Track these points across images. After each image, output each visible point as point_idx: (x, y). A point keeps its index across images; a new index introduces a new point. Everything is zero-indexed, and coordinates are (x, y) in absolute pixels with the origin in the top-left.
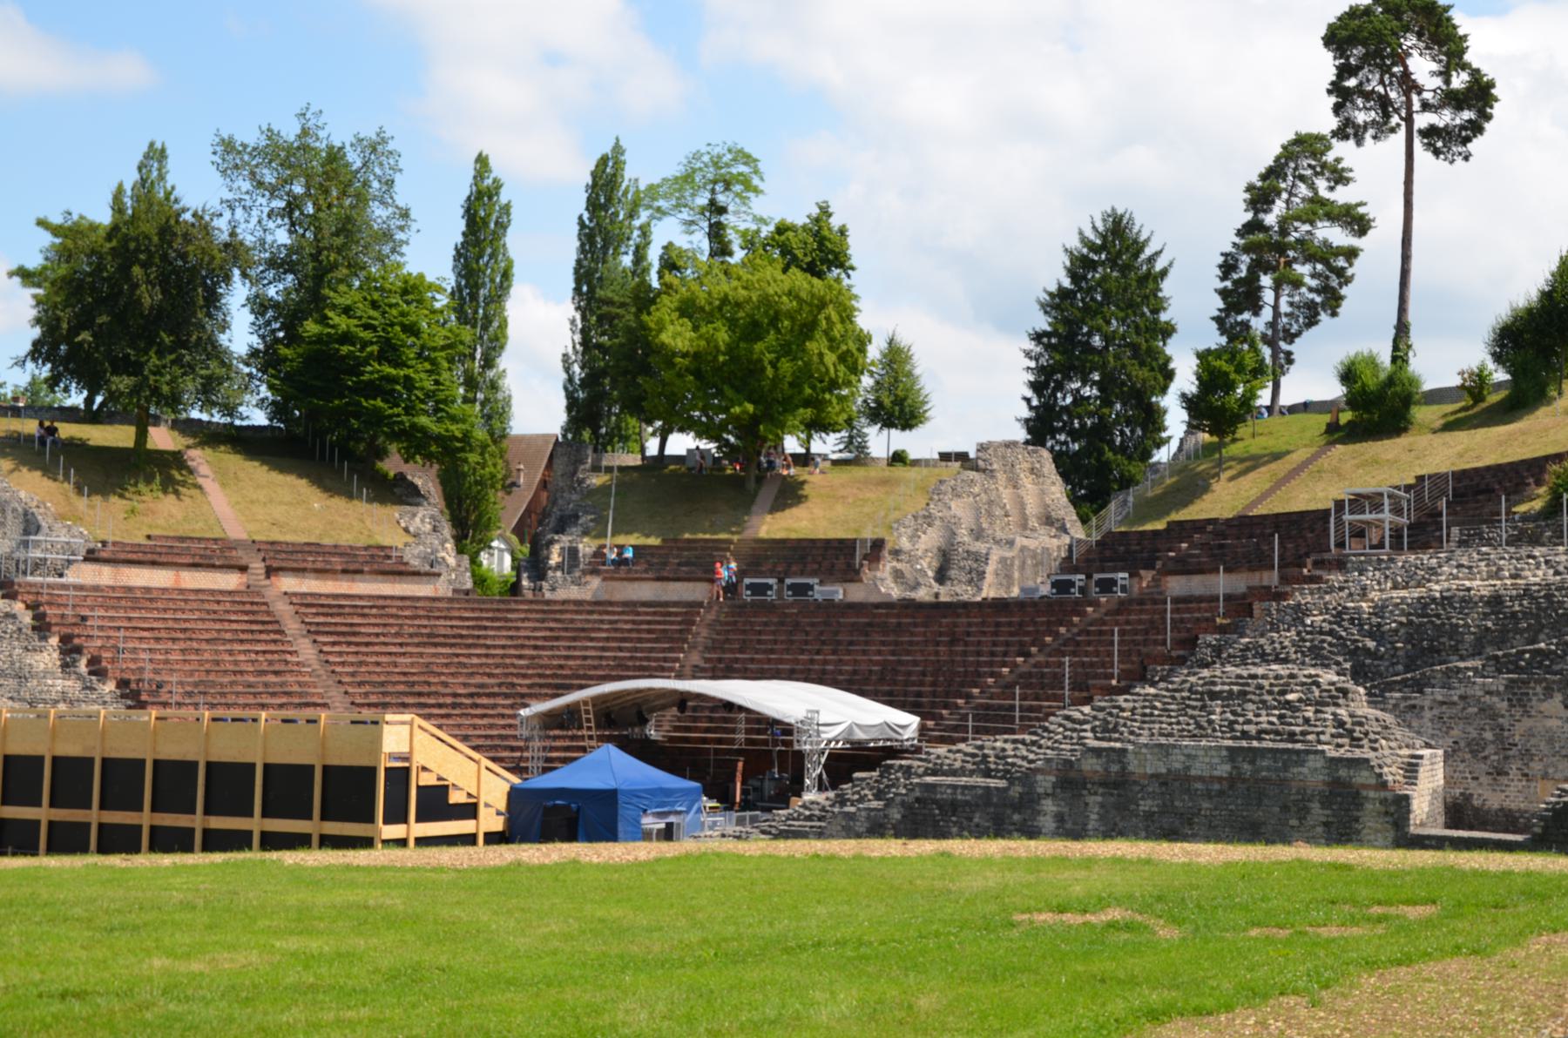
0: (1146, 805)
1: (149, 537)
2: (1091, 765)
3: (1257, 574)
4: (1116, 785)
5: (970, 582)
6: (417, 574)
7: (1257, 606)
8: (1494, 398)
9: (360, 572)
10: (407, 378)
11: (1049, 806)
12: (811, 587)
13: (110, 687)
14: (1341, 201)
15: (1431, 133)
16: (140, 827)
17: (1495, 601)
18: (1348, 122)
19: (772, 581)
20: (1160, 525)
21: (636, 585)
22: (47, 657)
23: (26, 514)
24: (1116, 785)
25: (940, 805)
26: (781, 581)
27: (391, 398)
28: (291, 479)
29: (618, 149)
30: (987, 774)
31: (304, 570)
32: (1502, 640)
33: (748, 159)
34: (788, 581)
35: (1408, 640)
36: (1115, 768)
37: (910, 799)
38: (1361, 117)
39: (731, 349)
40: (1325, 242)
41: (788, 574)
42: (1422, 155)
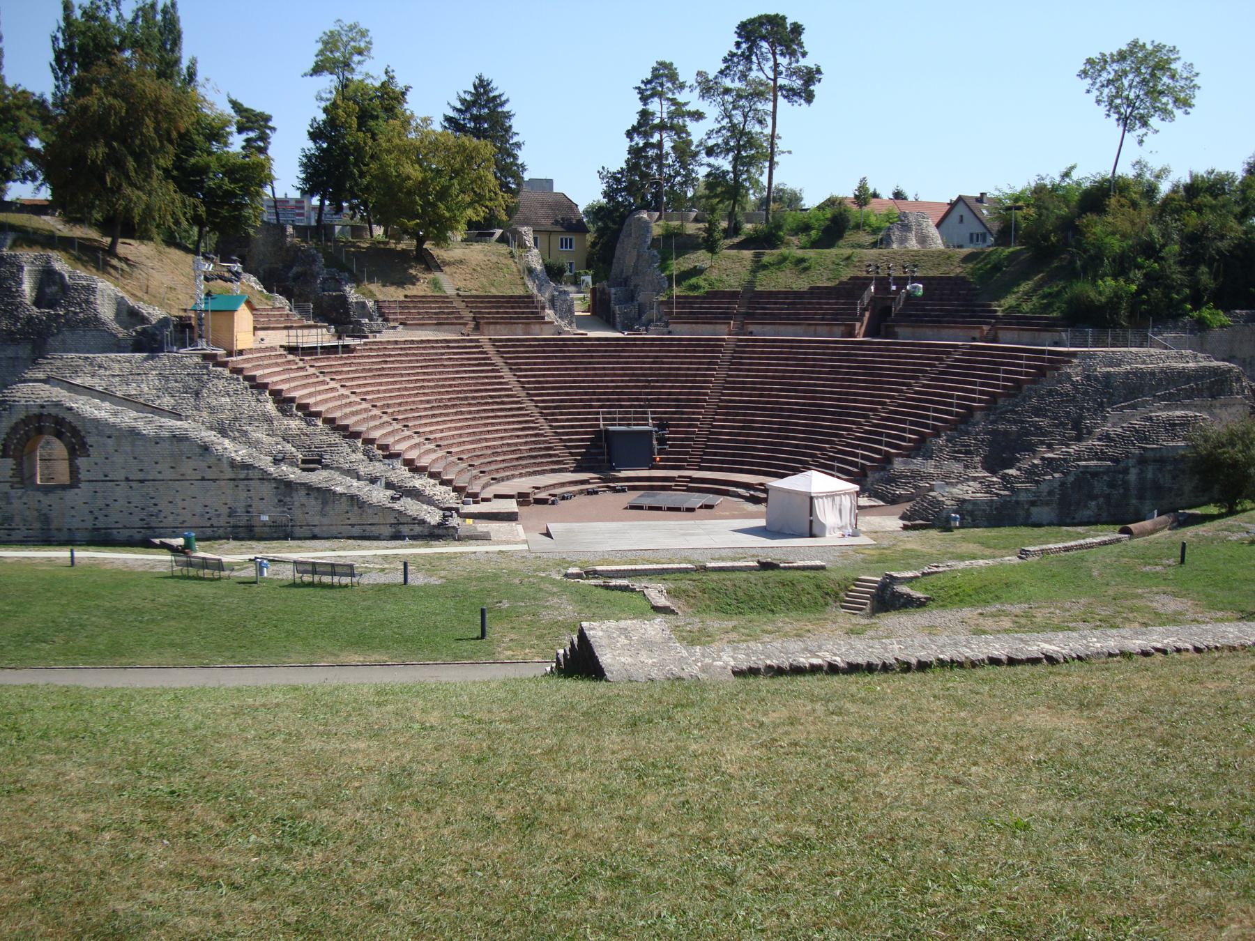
2: (1150, 454)
7: (1048, 373)
13: (320, 423)
22: (270, 407)
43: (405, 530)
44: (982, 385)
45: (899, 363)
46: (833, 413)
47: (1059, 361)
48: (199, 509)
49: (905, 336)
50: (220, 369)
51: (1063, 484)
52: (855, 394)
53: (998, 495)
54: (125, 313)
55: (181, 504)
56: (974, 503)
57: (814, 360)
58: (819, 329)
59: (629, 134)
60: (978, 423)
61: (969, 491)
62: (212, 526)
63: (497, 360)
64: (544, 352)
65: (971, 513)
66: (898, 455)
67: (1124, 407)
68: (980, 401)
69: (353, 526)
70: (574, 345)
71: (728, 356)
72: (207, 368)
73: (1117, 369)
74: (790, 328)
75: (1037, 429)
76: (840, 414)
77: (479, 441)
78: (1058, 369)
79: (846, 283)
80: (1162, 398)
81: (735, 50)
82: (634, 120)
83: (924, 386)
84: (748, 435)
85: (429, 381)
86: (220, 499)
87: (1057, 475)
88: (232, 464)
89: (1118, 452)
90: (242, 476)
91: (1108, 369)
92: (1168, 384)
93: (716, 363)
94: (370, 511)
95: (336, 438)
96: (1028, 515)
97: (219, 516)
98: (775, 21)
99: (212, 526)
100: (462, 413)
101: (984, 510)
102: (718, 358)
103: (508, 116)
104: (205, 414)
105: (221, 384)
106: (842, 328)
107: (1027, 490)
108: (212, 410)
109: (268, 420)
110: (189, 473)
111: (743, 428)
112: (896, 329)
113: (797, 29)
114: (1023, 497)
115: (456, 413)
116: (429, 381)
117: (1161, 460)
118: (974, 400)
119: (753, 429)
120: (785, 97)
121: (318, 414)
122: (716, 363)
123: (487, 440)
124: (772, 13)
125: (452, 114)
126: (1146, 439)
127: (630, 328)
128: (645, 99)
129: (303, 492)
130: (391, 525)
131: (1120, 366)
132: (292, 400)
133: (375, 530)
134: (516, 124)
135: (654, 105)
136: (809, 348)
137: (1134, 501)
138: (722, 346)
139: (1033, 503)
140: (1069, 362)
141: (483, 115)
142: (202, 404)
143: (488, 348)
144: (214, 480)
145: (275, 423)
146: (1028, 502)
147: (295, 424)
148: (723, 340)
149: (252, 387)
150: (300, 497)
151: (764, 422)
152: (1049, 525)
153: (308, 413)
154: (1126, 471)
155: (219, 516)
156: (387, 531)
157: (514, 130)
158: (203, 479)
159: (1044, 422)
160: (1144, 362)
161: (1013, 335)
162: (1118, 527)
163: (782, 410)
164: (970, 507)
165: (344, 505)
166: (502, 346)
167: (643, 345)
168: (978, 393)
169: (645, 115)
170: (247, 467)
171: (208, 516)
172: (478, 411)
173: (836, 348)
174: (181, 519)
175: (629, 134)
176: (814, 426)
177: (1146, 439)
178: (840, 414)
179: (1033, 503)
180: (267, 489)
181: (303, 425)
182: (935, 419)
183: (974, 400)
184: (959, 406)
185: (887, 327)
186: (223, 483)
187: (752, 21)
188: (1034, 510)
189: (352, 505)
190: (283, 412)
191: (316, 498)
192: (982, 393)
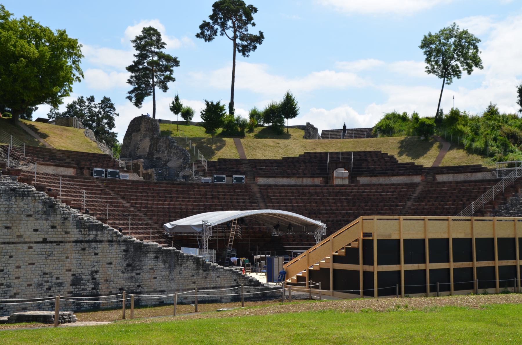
3: (301, 179)
14: (166, 53)
19: (104, 170)
48: (36, 279)
55: (14, 272)
90: (92, 237)
97: (60, 284)
110: (29, 235)
112: (358, 178)
129: (151, 256)
133: (217, 294)
144: (58, 243)
155: (60, 284)
156: (227, 293)
158: (45, 241)
165: (189, 268)
171: (46, 286)
174: (13, 291)
180: (115, 253)
186: (68, 245)
189: (198, 269)
191: (165, 262)
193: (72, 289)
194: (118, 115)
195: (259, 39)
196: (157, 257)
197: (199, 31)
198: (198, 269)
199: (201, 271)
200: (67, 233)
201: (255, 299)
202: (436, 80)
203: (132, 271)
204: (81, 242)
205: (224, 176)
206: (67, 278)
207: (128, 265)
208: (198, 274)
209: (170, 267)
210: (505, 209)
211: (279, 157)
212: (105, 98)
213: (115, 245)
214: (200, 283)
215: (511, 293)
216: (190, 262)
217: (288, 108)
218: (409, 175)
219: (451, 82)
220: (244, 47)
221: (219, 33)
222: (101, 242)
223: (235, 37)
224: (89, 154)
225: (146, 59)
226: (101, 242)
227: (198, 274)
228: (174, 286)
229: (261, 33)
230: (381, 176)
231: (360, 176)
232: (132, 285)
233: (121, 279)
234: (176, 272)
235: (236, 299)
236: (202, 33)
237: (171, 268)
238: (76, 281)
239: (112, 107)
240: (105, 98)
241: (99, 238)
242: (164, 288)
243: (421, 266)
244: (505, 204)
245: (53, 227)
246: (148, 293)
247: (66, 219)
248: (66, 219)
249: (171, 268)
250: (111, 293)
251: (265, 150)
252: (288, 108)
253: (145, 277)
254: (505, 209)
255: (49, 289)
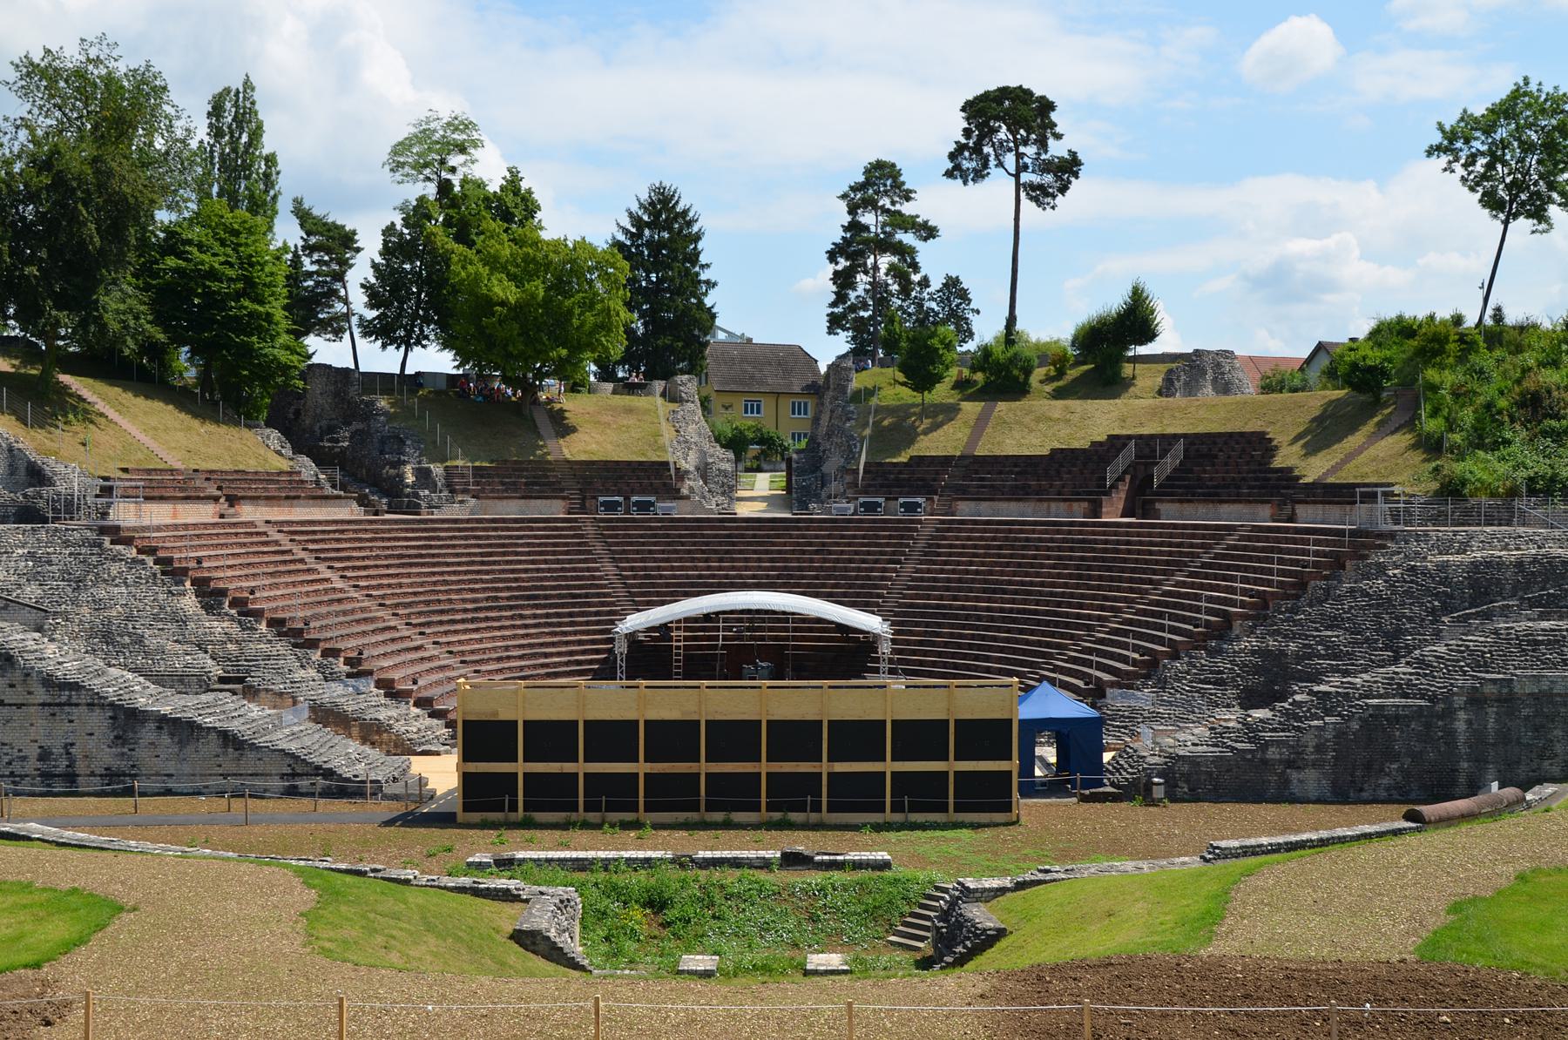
0: (1525, 712)
1: (125, 470)
4: (1506, 701)
5: (723, 494)
6: (327, 498)
7: (1348, 563)
8: (1073, 374)
9: (298, 497)
10: (268, 314)
11: (1462, 715)
12: (652, 504)
13: (263, 627)
15: (1032, 187)
16: (759, 774)
17: (1519, 564)
18: (957, 167)
20: (903, 458)
21: (505, 502)
22: (189, 603)
23: (11, 449)
24: (1506, 701)
25: (1387, 718)
26: (627, 498)
27: (263, 333)
28: (158, 405)
29: (248, 85)
30: (1406, 696)
31: (258, 498)
32: (1527, 589)
33: (467, 126)
34: (634, 498)
35: (1471, 587)
36: (1505, 691)
37: (1366, 715)
38: (966, 165)
39: (547, 301)
40: (900, 242)
41: (633, 492)
42: (1025, 203)
43: (303, 783)
44: (1245, 580)
45: (1151, 553)
46: (1048, 624)
47: (1364, 546)
49: (1171, 514)
50: (118, 547)
51: (1340, 734)
52: (1083, 596)
53: (1233, 748)
54: (22, 471)
56: (1192, 761)
57: (1037, 548)
58: (1053, 505)
59: (832, 257)
60: (1238, 638)
61: (1191, 739)
62: (12, 774)
63: (599, 548)
64: (668, 536)
65: (1187, 777)
66: (1112, 685)
67: (1469, 616)
68: (1243, 605)
69: (225, 776)
70: (712, 528)
71: (921, 543)
72: (100, 545)
73: (1459, 558)
74: (1013, 505)
75: (1328, 648)
76: (1057, 625)
77: (534, 656)
78: (1366, 557)
79: (1100, 444)
80: (1533, 604)
81: (963, 141)
82: (837, 235)
83: (1178, 584)
84: (925, 654)
85: (487, 572)
86: (30, 734)
87: (1333, 720)
88: (49, 681)
89: (1437, 685)
90: (64, 699)
91: (1445, 558)
92: (1546, 581)
93: (903, 554)
94: (251, 755)
95: (281, 647)
96: (1286, 782)
98: (1021, 95)
99: (12, 774)
100: (522, 617)
101: (1210, 774)
102: (908, 546)
103: (697, 238)
104: (85, 610)
105: (115, 568)
106: (1086, 504)
107: (1279, 743)
108: (98, 605)
109: (181, 620)
111: (921, 643)
112: (1158, 506)
113: (1047, 106)
114: (1273, 753)
115: (512, 618)
116: (487, 572)
117: (1507, 699)
118: (1233, 603)
119: (934, 644)
120: (1031, 198)
121: (258, 614)
122: (903, 554)
123: (546, 655)
124: (1013, 84)
125: (621, 237)
126: (1486, 664)
127: (804, 506)
128: (852, 210)
129: (153, 725)
130: (282, 776)
131: (1464, 552)
132: (223, 593)
134: (708, 250)
135: (868, 218)
136: (1034, 532)
137: (1466, 765)
138: (916, 530)
139: (1290, 764)
140: (1384, 547)
141: (664, 240)
142: (83, 596)
143: (590, 530)
144: (19, 706)
145: (191, 625)
146: (1280, 761)
147: (218, 627)
148: (920, 522)
149: (163, 573)
150: (147, 733)
151: (952, 635)
152: (1318, 801)
153: (245, 610)
154: (1449, 713)
155: (24, 758)
156: (278, 784)
157: (703, 259)
159: (1336, 636)
160: (1506, 547)
161: (1319, 510)
162: (1405, 808)
163: (979, 618)
164: (1186, 768)
165: (213, 743)
166: (608, 531)
167: (808, 529)
168: (1240, 593)
169: (855, 227)
170: (76, 687)
172: (548, 616)
173: (1069, 533)
175: (832, 257)
176: (983, 638)
177: (1486, 666)
178: (1057, 625)
179: (1290, 764)
180: (98, 721)
181: (235, 630)
182: (1173, 630)
183: (1233, 603)
184: (1209, 612)
185: (1145, 502)
186: (32, 709)
187: (985, 97)
188: (1294, 775)
190: (208, 608)
191: (172, 735)
192: (1244, 592)
193: (39, 765)
194: (978, 312)
195: (1069, 168)
196: (160, 728)
197: (950, 165)
198: (225, 746)
199: (230, 750)
200: (30, 693)
201: (327, 793)
202: (1488, 225)
203: (123, 745)
204: (50, 705)
205: (880, 500)
206: (33, 751)
207: (117, 737)
208: (225, 754)
209: (180, 742)
210: (1287, 610)
211: (1045, 452)
212: (949, 278)
213: (98, 710)
214: (229, 767)
215: (1309, 802)
216: (213, 736)
217: (1135, 321)
218: (1250, 502)
219: (1551, 226)
220: (1041, 187)
221: (992, 162)
222: (77, 705)
223: (1021, 168)
224: (640, 463)
225: (271, 407)
226: (77, 705)
227: (225, 754)
228: (187, 769)
229: (1073, 154)
230: (1199, 501)
231: (1162, 501)
232: (123, 765)
233: (106, 756)
234: (189, 749)
235: (292, 792)
236: (957, 167)
237: (182, 744)
238: (45, 755)
239: (964, 295)
240: (949, 278)
241: (74, 700)
242: (172, 771)
243: (568, 767)
244: (1297, 597)
245: (12, 686)
246: (148, 776)
247: (28, 675)
248: (28, 675)
249: (182, 744)
250: (93, 774)
251: (1031, 431)
252: (1135, 321)
253: (143, 754)
254: (1287, 610)
255: (9, 763)
